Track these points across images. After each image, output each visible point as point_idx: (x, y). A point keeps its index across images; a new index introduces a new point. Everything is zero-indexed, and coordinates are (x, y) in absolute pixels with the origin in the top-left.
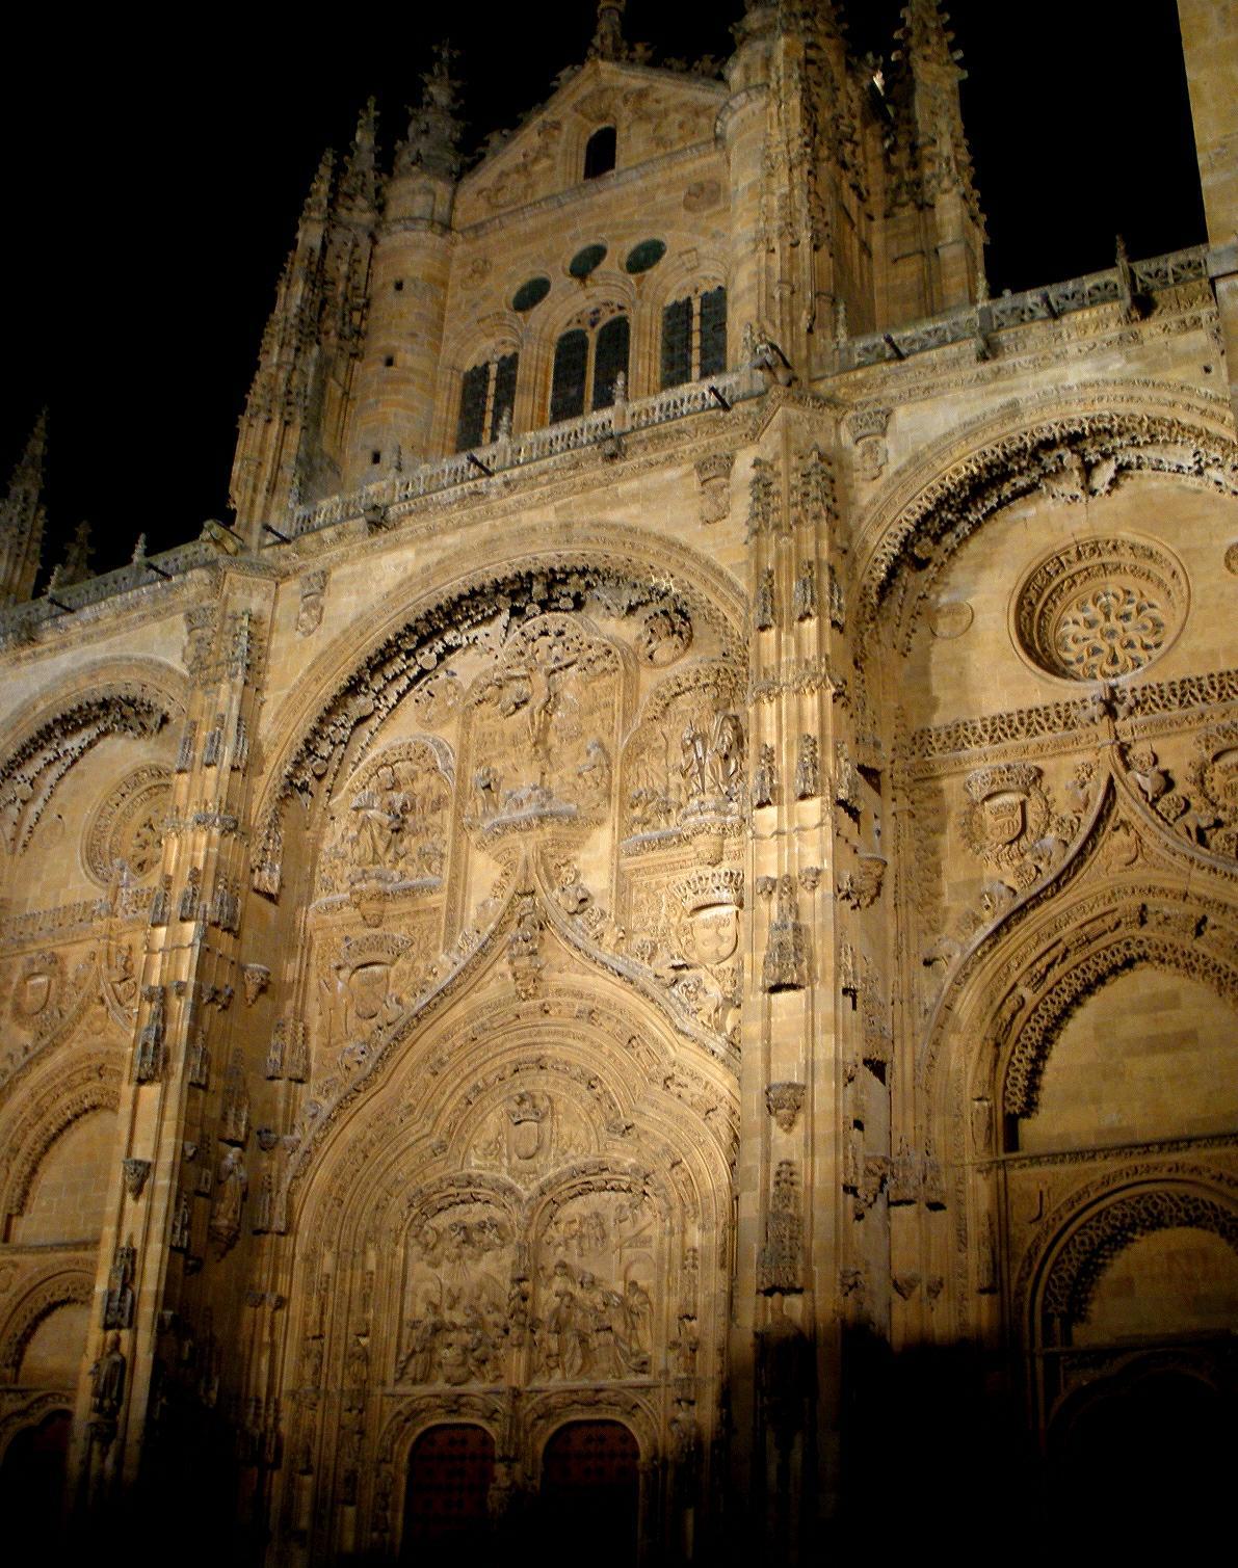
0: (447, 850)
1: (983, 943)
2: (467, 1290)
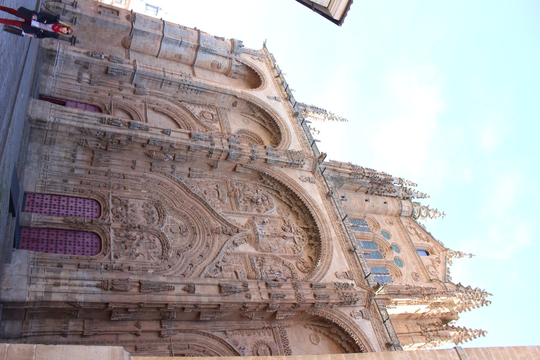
0: (247, 212)
1: (231, 346)
2: (136, 214)
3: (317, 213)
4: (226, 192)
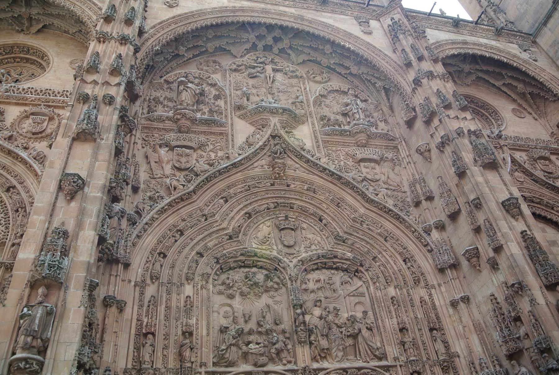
2: (254, 313)
3: (247, 14)
4: (172, 135)
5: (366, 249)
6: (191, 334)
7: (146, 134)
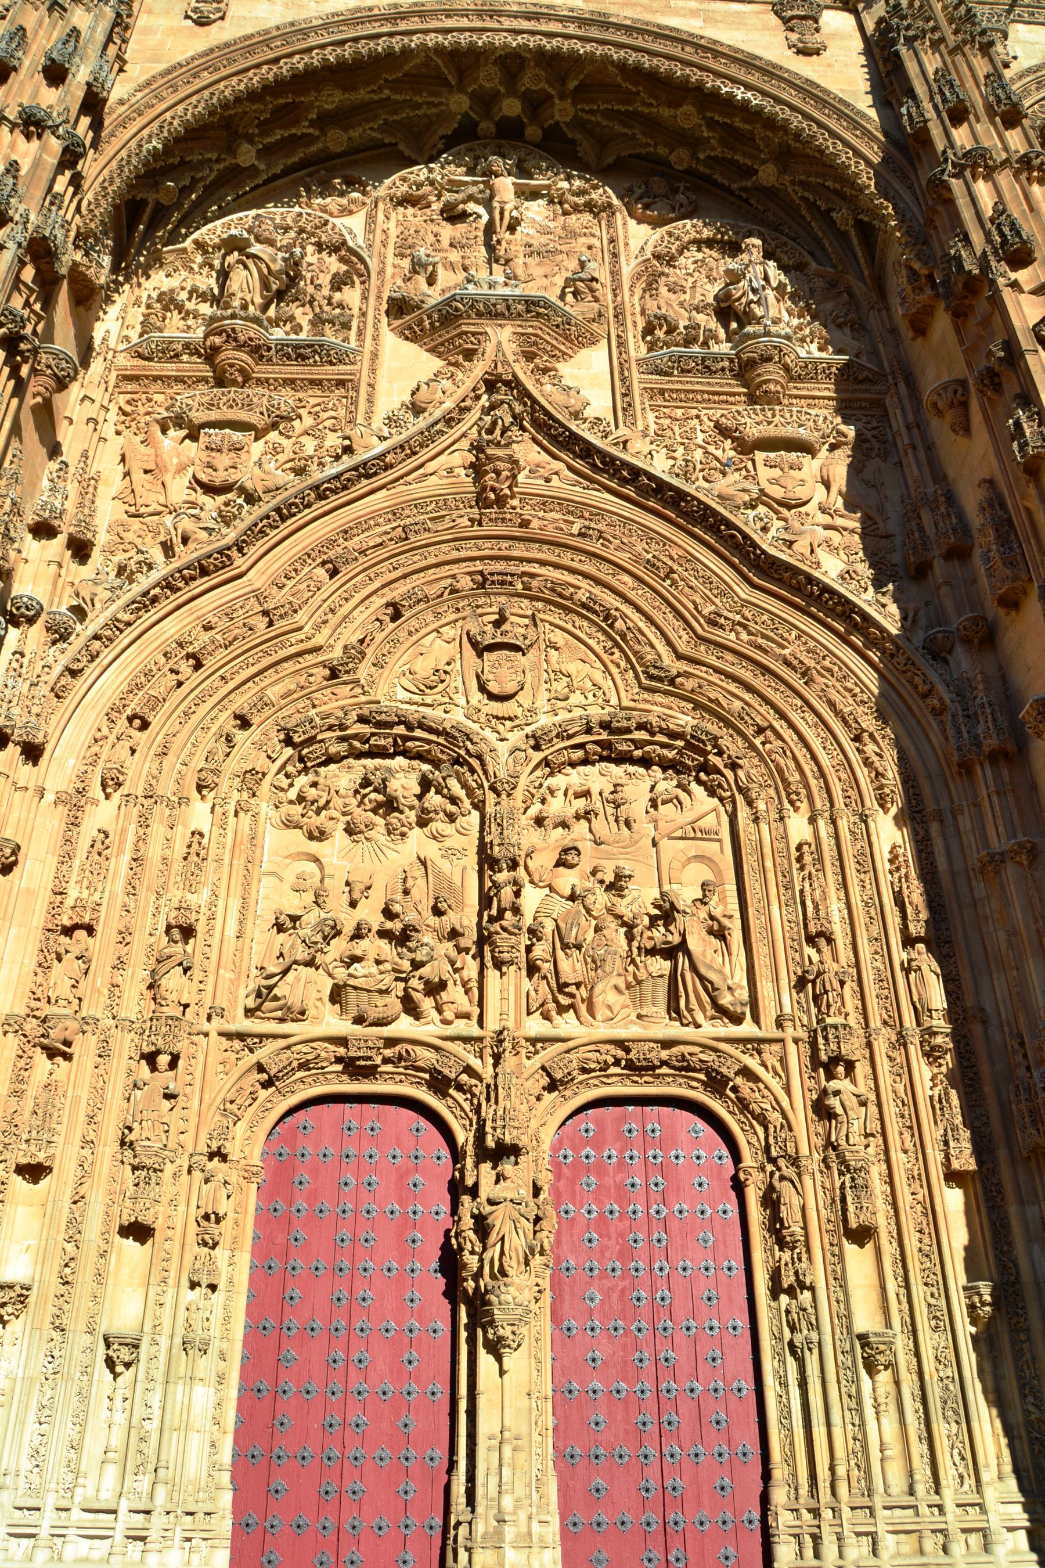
5: (737, 705)
6: (188, 932)
7: (129, 396)
